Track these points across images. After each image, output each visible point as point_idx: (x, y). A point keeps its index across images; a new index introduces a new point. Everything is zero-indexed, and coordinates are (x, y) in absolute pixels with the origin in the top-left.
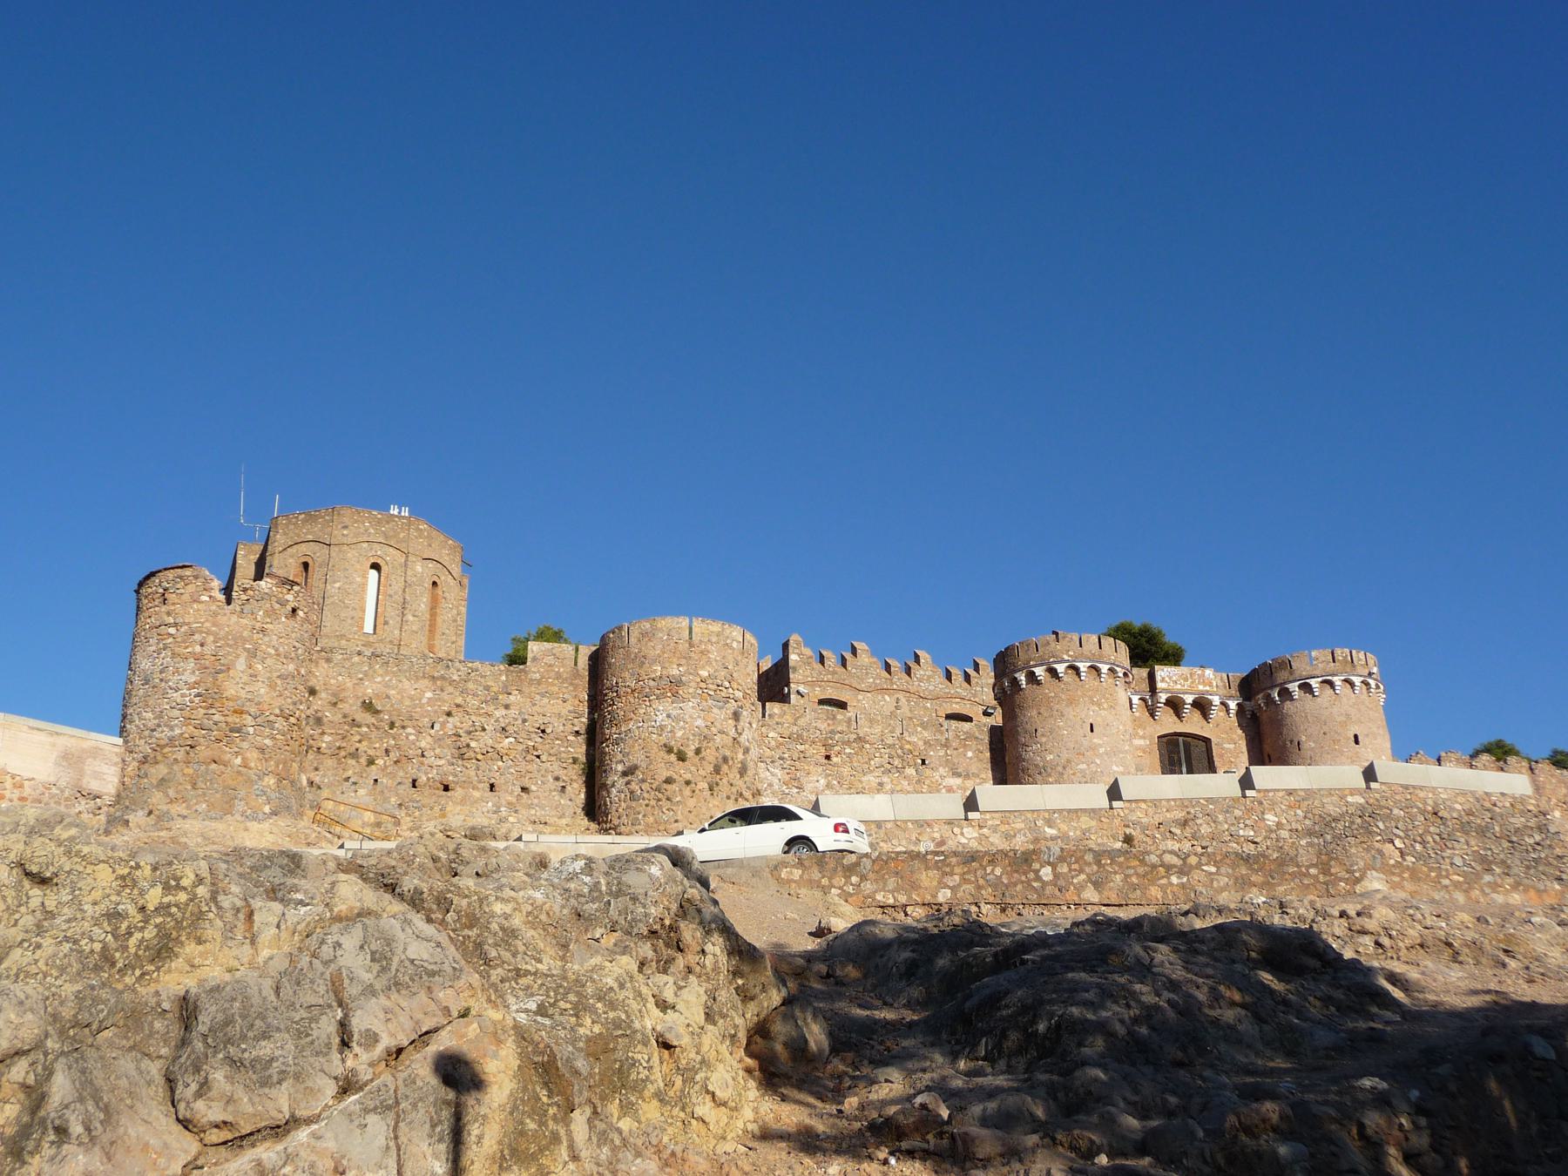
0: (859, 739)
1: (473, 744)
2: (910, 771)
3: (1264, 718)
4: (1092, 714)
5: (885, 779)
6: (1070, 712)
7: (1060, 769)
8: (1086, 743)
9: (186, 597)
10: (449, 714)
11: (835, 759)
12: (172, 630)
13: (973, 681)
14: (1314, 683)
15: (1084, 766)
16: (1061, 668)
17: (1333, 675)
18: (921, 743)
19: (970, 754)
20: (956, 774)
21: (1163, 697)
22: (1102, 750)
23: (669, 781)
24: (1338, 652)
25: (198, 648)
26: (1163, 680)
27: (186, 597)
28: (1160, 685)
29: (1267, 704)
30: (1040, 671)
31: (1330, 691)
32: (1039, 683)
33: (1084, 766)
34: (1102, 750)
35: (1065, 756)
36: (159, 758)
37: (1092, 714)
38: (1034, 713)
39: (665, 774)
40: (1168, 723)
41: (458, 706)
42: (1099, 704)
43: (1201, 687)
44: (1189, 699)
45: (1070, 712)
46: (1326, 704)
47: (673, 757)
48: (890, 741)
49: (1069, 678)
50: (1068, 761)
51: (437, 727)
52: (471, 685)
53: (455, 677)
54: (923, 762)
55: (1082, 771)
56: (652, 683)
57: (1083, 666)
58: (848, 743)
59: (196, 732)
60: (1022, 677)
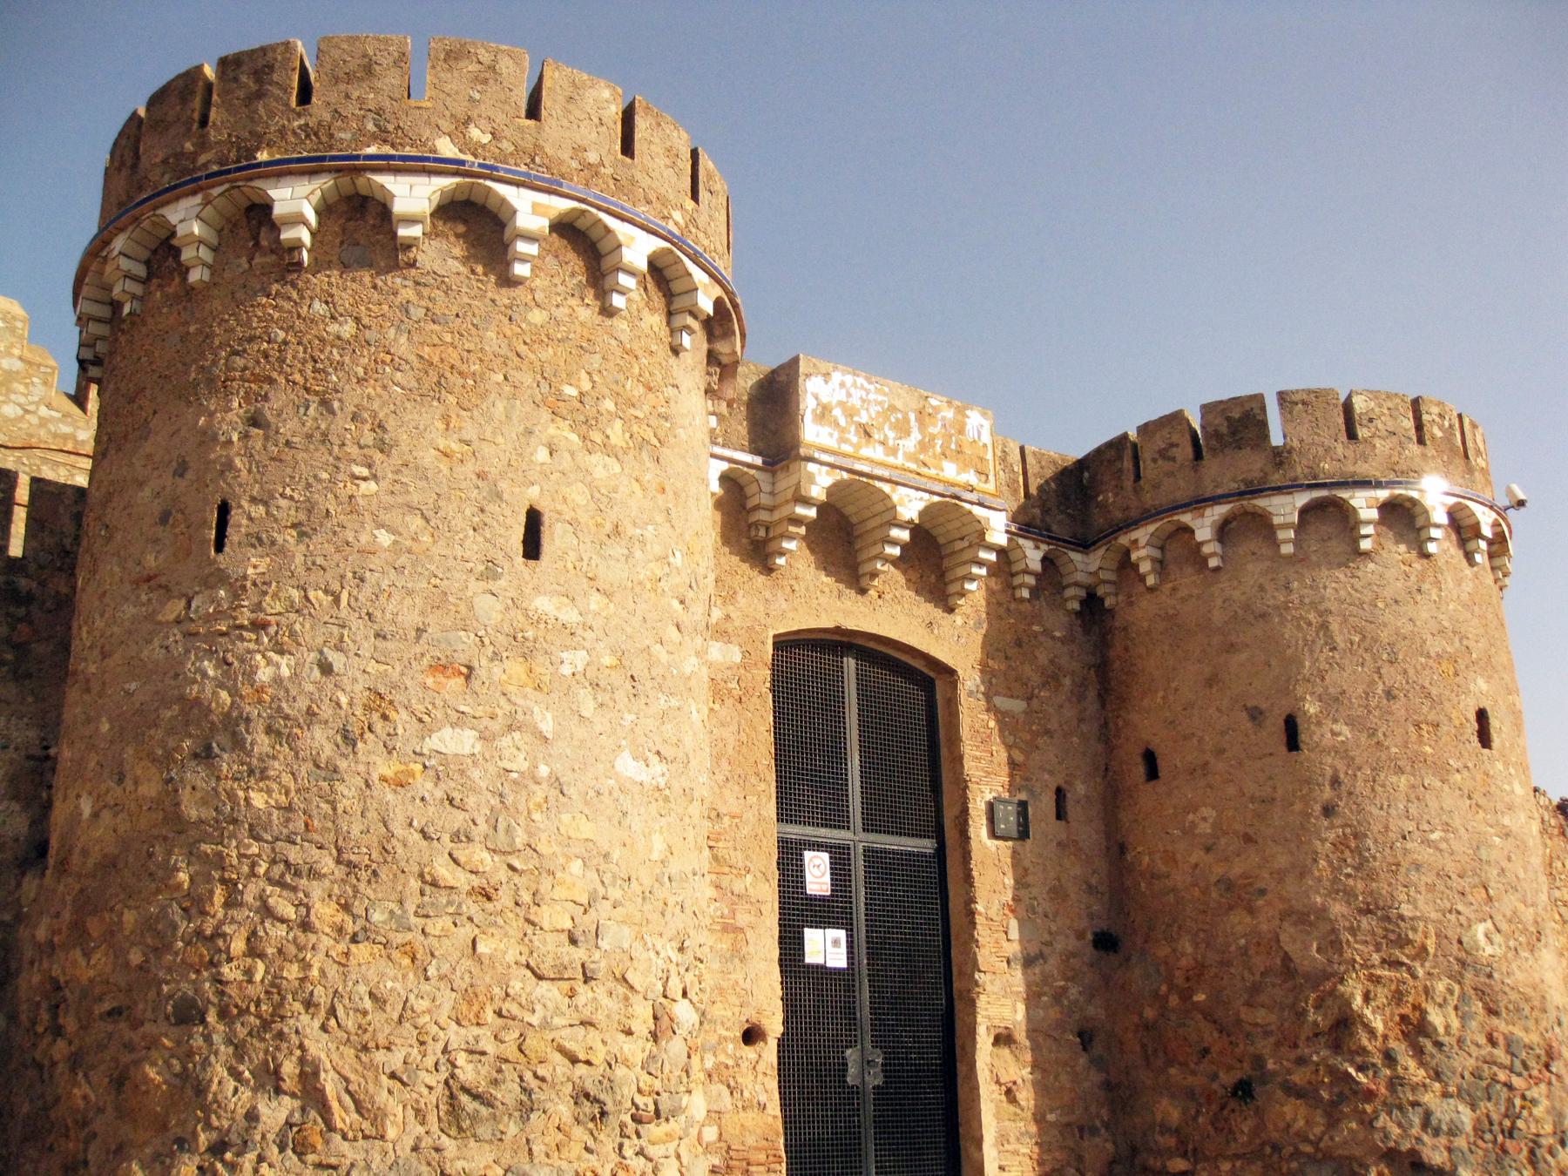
3: (1141, 613)
4: (544, 461)
6: (425, 434)
8: (489, 609)
16: (413, 196)
21: (819, 482)
22: (574, 660)
26: (824, 413)
28: (812, 433)
29: (1161, 565)
32: (286, 263)
33: (455, 741)
34: (574, 660)
35: (358, 671)
37: (544, 461)
38: (230, 418)
40: (811, 599)
42: (587, 423)
43: (950, 471)
44: (910, 505)
45: (425, 434)
46: (1396, 587)
49: (441, 257)
57: (531, 211)
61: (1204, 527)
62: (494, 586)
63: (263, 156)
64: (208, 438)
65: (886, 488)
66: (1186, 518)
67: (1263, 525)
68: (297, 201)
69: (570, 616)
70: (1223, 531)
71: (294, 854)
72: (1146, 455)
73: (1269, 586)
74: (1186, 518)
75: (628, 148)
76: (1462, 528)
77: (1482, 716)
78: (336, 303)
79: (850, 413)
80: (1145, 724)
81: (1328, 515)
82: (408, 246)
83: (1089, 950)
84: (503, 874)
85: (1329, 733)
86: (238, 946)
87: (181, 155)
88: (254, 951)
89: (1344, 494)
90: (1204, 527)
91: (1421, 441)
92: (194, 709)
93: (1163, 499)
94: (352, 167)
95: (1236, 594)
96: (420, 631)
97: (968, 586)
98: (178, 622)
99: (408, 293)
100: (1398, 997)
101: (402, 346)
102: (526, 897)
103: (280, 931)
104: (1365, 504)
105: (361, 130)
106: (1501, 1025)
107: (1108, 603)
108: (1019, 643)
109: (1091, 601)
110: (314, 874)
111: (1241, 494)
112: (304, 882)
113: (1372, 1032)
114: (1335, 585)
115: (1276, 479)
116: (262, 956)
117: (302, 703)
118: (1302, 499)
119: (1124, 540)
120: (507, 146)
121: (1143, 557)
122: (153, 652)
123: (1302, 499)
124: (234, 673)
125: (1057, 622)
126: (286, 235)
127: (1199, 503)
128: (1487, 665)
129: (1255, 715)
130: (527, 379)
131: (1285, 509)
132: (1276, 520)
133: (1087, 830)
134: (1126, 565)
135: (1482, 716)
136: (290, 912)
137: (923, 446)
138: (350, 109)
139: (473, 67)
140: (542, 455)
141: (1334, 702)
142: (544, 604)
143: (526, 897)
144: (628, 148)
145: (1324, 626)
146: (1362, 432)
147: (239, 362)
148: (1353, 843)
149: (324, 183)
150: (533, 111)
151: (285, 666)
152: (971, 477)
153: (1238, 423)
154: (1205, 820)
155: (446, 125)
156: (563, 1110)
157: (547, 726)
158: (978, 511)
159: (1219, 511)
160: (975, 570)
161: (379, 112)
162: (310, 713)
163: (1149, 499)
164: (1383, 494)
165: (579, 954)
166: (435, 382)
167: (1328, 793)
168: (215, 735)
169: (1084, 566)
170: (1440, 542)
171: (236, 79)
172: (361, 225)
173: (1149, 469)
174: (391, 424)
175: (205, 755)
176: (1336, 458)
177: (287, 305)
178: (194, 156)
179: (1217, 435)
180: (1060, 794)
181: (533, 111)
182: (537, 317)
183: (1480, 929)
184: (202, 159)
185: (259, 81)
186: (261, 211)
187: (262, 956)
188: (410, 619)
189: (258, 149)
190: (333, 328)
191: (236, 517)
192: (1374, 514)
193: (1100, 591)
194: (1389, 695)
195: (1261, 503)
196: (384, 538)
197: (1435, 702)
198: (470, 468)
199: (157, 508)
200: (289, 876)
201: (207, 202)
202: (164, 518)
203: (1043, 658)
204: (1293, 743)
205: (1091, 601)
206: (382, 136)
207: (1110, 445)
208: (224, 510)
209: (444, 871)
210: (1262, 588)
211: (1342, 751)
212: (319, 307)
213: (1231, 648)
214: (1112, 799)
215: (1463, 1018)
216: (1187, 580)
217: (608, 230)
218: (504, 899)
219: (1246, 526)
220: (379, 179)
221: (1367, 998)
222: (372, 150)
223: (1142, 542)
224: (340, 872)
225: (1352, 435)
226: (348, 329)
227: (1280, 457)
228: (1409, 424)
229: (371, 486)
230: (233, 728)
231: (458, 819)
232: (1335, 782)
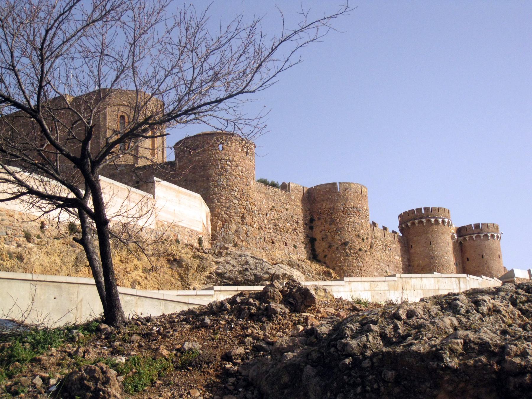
1: (280, 225)
2: (387, 252)
3: (467, 244)
9: (232, 149)
10: (271, 210)
12: (229, 163)
23: (360, 250)
25: (241, 173)
27: (232, 149)
32: (432, 225)
33: (446, 258)
36: (232, 221)
39: (358, 247)
41: (273, 207)
47: (361, 241)
48: (382, 239)
51: (268, 215)
52: (276, 198)
53: (271, 194)
56: (351, 209)
59: (245, 211)
61: (474, 236)
64: (428, 237)
67: (480, 236)
68: (433, 220)
70: (476, 237)
76: (498, 237)
78: (435, 228)
80: (467, 255)
81: (486, 236)
85: (486, 257)
90: (474, 236)
92: (431, 256)
94: (437, 218)
104: (489, 235)
109: (461, 243)
114: (486, 242)
121: (467, 239)
122: (426, 251)
124: (433, 253)
125: (458, 245)
127: (474, 234)
128: (500, 250)
131: (482, 235)
133: (461, 266)
134: (465, 238)
141: (486, 254)
148: (488, 267)
153: (477, 226)
154: (474, 265)
159: (475, 235)
163: (468, 233)
166: (442, 233)
168: (433, 257)
169: (461, 239)
170: (495, 238)
172: (437, 221)
176: (486, 230)
186: (431, 221)
200: (439, 266)
205: (461, 243)
211: (487, 258)
214: (463, 262)
216: (472, 242)
219: (478, 236)
223: (467, 237)
227: (481, 230)
230: (434, 257)
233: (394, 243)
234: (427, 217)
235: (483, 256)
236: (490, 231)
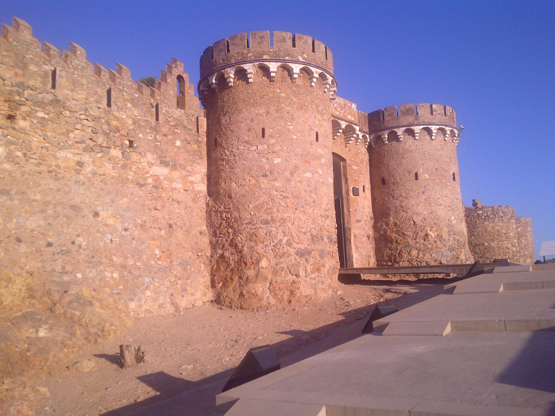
0: (56, 102)
2: (116, 153)
5: (86, 158)
7: (287, 174)
11: (21, 123)
13: (118, 80)
14: (434, 128)
15: (309, 175)
16: (296, 68)
17: (447, 126)
18: (130, 121)
19: (178, 143)
20: (164, 163)
24: (448, 108)
30: (273, 67)
31: (441, 137)
33: (309, 175)
38: (262, 111)
48: (94, 112)
50: (296, 167)
54: (131, 142)
55: (308, 179)
58: (41, 104)
60: (231, 74)
62: (312, 146)
63: (265, 57)
65: (340, 121)
66: (396, 130)
69: (322, 152)
71: (284, 194)
72: (386, 114)
73: (413, 145)
74: (396, 130)
75: (326, 59)
77: (454, 174)
79: (333, 105)
82: (295, 78)
83: (369, 219)
84: (316, 199)
86: (275, 211)
87: (243, 54)
88: (278, 211)
89: (430, 126)
91: (445, 116)
93: (390, 126)
95: (405, 147)
96: (302, 155)
97: (350, 142)
98: (255, 151)
99: (294, 88)
100: (436, 231)
101: (295, 100)
102: (320, 203)
103: (282, 208)
105: (284, 53)
106: (457, 237)
107: (374, 146)
108: (356, 154)
110: (288, 198)
111: (408, 126)
112: (286, 200)
113: (432, 237)
115: (416, 122)
116: (280, 212)
117: (283, 168)
118: (421, 127)
119: (380, 133)
120: (310, 59)
123: (421, 127)
126: (272, 74)
127: (399, 127)
129: (409, 172)
130: (314, 106)
132: (416, 132)
135: (454, 174)
136: (283, 204)
137: (345, 112)
138: (282, 49)
139: (303, 41)
140: (317, 122)
142: (319, 150)
143: (320, 203)
144: (326, 59)
145: (424, 154)
146: (434, 113)
147: (263, 100)
149: (279, 64)
150: (313, 51)
151: (279, 160)
152: (353, 119)
155: (300, 53)
156: (326, 240)
157: (320, 173)
158: (354, 126)
160: (352, 139)
161: (287, 50)
162: (285, 169)
164: (438, 127)
165: (327, 213)
166: (301, 107)
167: (423, 189)
171: (255, 38)
173: (386, 118)
174: (294, 115)
175: (265, 176)
177: (272, 89)
178: (247, 54)
179: (403, 112)
180: (364, 186)
181: (313, 51)
182: (315, 94)
183: (453, 218)
184: (250, 55)
185: (261, 39)
187: (280, 212)
188: (300, 152)
189: (264, 54)
190: (281, 94)
191: (266, 131)
192: (435, 131)
193: (372, 144)
194: (436, 169)
195: (412, 127)
196: (295, 137)
197: (446, 171)
198: (307, 124)
199: (247, 128)
201: (254, 65)
202: (249, 130)
203: (361, 158)
204: (417, 178)
206: (288, 55)
207: (376, 111)
208: (263, 130)
209: (308, 198)
210: (411, 146)
212: (278, 90)
213: (404, 158)
215: (450, 235)
217: (326, 76)
218: (317, 203)
220: (291, 65)
221: (431, 230)
222: (287, 58)
224: (292, 198)
225: (432, 114)
226: (283, 95)
228: (443, 112)
229: (292, 127)
231: (310, 189)
232: (425, 187)
233: (156, 130)
234: (258, 58)
235: (416, 174)
236: (435, 121)
